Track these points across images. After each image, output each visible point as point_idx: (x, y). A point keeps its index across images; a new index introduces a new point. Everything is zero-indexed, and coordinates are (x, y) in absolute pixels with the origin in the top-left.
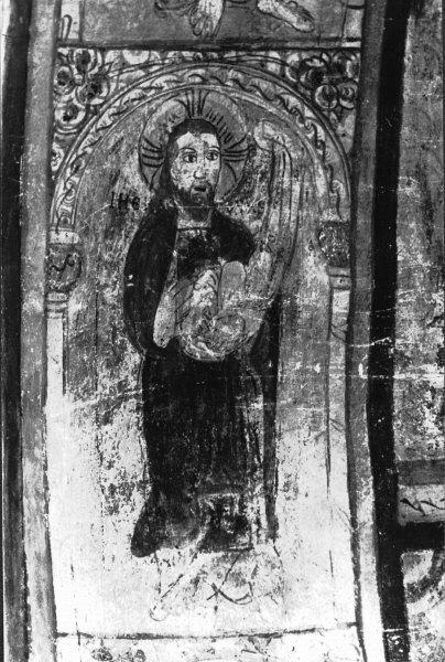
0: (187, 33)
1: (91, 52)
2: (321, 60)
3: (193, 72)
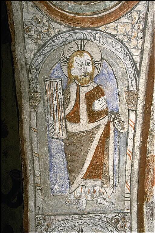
0: (75, 211)
1: (47, 216)
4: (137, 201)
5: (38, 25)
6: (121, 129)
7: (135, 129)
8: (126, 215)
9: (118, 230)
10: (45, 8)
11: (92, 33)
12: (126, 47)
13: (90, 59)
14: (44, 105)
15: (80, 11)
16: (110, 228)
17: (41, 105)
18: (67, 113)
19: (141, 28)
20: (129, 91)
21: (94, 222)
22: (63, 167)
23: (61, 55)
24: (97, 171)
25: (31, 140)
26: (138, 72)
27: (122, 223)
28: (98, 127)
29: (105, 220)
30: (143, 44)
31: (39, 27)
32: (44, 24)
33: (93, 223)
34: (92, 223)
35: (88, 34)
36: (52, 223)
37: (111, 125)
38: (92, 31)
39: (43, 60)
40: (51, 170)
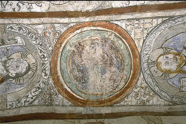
5: (140, 95)
10: (128, 90)
11: (143, 57)
12: (152, 30)
13: (162, 56)
15: (129, 66)
19: (137, 22)
23: (160, 78)
26: (171, 18)
30: (148, 18)
31: (141, 94)
32: (139, 91)
35: (144, 59)
38: (142, 57)
39: (165, 92)
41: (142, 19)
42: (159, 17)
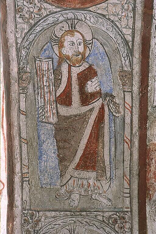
0: (66, 207)
1: (34, 213)
2: (116, 214)
3: (71, 219)
4: (138, 198)
5: (30, 6)
6: (117, 113)
7: (132, 113)
8: (126, 214)
9: (116, 231)
11: (82, 13)
12: (117, 27)
13: (81, 38)
14: (34, 86)
16: (108, 229)
17: (30, 87)
18: (58, 95)
19: (131, 8)
20: (122, 71)
21: (88, 221)
22: (53, 155)
23: (52, 34)
24: (90, 161)
25: (19, 124)
26: (131, 52)
27: (121, 223)
28: (91, 110)
29: (101, 220)
30: (134, 23)
31: (31, 7)
32: (35, 4)
33: (87, 222)
34: (86, 222)
35: (80, 15)
36: (40, 221)
37: (106, 109)
38: (82, 12)
39: (33, 40)
40: (40, 158)
41: (134, 14)
42: (133, 38)
